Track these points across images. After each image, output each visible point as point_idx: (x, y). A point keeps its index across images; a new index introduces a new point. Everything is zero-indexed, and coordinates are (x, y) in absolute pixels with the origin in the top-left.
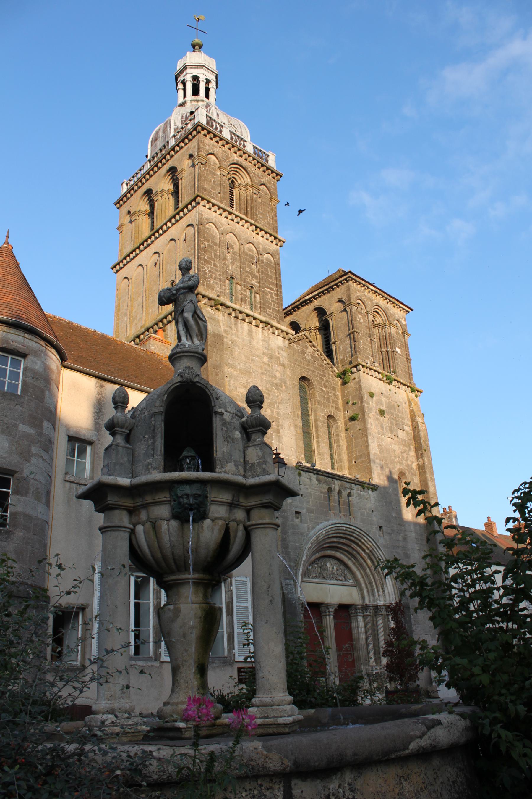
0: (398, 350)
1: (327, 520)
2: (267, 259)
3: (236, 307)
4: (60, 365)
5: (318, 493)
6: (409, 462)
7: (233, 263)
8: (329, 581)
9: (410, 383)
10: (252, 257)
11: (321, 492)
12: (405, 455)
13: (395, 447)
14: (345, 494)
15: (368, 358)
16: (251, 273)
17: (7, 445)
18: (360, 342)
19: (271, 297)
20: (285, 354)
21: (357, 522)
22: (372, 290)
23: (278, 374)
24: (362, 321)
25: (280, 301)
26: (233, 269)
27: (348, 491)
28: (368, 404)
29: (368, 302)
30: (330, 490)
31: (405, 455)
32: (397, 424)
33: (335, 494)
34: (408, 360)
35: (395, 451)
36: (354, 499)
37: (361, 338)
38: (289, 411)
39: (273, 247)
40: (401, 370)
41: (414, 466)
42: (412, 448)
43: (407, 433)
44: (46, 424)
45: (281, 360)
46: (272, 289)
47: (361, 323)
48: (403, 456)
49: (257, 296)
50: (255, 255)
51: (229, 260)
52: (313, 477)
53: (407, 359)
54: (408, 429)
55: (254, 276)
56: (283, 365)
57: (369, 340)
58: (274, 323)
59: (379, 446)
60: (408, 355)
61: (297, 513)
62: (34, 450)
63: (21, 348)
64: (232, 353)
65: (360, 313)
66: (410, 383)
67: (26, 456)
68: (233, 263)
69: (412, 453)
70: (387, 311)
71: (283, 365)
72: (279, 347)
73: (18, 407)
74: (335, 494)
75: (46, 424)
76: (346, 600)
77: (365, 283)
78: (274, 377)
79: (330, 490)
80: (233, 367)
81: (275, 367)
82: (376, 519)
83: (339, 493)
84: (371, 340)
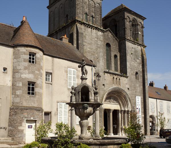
0: (140, 33)
1: (112, 87)
2: (98, 6)
5: (110, 79)
6: (140, 69)
8: (111, 103)
9: (143, 44)
10: (93, 5)
11: (111, 79)
12: (138, 67)
13: (135, 65)
14: (118, 79)
15: (129, 36)
18: (126, 31)
19: (99, 19)
20: (102, 37)
21: (121, 87)
22: (132, 13)
23: (99, 44)
24: (128, 24)
27: (119, 78)
28: (128, 51)
31: (138, 67)
32: (136, 57)
35: (135, 66)
36: (121, 81)
37: (127, 30)
40: (140, 40)
41: (141, 70)
42: (141, 65)
43: (140, 60)
45: (101, 39)
46: (99, 16)
47: (128, 25)
48: (138, 68)
49: (94, 19)
50: (94, 4)
53: (142, 36)
56: (101, 41)
57: (130, 30)
58: (99, 28)
65: (128, 21)
66: (143, 44)
69: (141, 66)
70: (137, 19)
71: (101, 41)
72: (100, 35)
78: (99, 45)
79: (113, 78)
83: (116, 78)
84: (130, 30)
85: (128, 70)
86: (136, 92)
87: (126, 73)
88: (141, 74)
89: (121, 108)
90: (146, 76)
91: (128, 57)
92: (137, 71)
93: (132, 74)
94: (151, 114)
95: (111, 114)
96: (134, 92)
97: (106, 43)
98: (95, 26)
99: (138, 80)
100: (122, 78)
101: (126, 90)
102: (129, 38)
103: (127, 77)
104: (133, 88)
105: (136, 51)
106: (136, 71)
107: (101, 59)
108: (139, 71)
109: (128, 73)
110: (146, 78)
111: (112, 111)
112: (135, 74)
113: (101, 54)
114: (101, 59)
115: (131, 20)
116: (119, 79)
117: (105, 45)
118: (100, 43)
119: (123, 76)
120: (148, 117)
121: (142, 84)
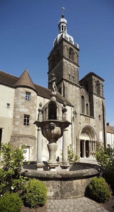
3: (70, 81)
4: (37, 95)
7: (69, 71)
14: (89, 119)
16: (73, 73)
17: (28, 110)
20: (79, 91)
21: (91, 125)
25: (78, 80)
26: (70, 73)
29: (96, 79)
30: (86, 118)
33: (87, 119)
34: (103, 92)
38: (79, 103)
39: (77, 67)
41: (102, 114)
44: (35, 106)
50: (74, 69)
51: (69, 71)
52: (83, 116)
54: (102, 107)
55: (73, 74)
56: (78, 93)
58: (77, 84)
59: (96, 110)
60: (103, 91)
61: (80, 123)
62: (33, 111)
63: (30, 92)
64: (69, 91)
67: (31, 113)
68: (69, 71)
69: (102, 112)
73: (30, 103)
74: (87, 119)
75: (35, 106)
76: (88, 140)
77: (95, 75)
79: (86, 118)
80: (69, 94)
81: (77, 94)
82: (94, 124)
83: (88, 119)
85: (95, 114)
86: (99, 128)
87: (93, 116)
88: (102, 117)
89: (91, 139)
90: (105, 118)
91: (95, 105)
92: (100, 114)
93: (97, 117)
94: (108, 143)
95: (85, 143)
96: (98, 128)
97: (81, 96)
98: (75, 83)
99: (101, 120)
100: (91, 119)
101: (93, 127)
102: (95, 92)
103: (94, 118)
104: (97, 126)
105: (99, 102)
106: (99, 114)
107: (78, 105)
108: (101, 114)
109: (94, 116)
110: (105, 119)
111: (85, 141)
112: (98, 116)
113: (78, 102)
114: (78, 105)
115: (96, 81)
116: (89, 119)
117: (81, 97)
118: (77, 95)
119: (92, 118)
120: (107, 145)
121: (103, 123)
